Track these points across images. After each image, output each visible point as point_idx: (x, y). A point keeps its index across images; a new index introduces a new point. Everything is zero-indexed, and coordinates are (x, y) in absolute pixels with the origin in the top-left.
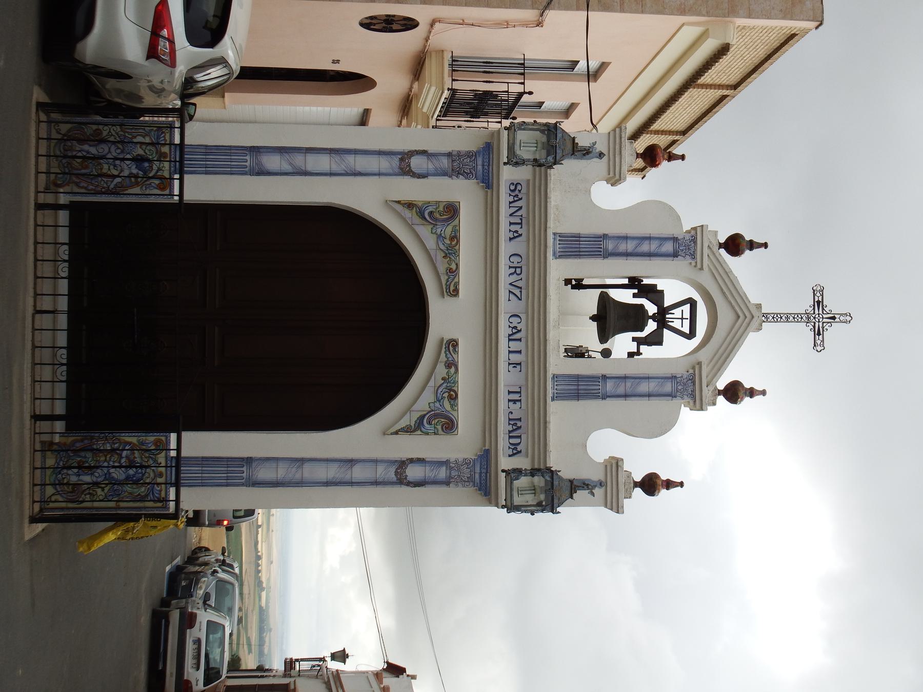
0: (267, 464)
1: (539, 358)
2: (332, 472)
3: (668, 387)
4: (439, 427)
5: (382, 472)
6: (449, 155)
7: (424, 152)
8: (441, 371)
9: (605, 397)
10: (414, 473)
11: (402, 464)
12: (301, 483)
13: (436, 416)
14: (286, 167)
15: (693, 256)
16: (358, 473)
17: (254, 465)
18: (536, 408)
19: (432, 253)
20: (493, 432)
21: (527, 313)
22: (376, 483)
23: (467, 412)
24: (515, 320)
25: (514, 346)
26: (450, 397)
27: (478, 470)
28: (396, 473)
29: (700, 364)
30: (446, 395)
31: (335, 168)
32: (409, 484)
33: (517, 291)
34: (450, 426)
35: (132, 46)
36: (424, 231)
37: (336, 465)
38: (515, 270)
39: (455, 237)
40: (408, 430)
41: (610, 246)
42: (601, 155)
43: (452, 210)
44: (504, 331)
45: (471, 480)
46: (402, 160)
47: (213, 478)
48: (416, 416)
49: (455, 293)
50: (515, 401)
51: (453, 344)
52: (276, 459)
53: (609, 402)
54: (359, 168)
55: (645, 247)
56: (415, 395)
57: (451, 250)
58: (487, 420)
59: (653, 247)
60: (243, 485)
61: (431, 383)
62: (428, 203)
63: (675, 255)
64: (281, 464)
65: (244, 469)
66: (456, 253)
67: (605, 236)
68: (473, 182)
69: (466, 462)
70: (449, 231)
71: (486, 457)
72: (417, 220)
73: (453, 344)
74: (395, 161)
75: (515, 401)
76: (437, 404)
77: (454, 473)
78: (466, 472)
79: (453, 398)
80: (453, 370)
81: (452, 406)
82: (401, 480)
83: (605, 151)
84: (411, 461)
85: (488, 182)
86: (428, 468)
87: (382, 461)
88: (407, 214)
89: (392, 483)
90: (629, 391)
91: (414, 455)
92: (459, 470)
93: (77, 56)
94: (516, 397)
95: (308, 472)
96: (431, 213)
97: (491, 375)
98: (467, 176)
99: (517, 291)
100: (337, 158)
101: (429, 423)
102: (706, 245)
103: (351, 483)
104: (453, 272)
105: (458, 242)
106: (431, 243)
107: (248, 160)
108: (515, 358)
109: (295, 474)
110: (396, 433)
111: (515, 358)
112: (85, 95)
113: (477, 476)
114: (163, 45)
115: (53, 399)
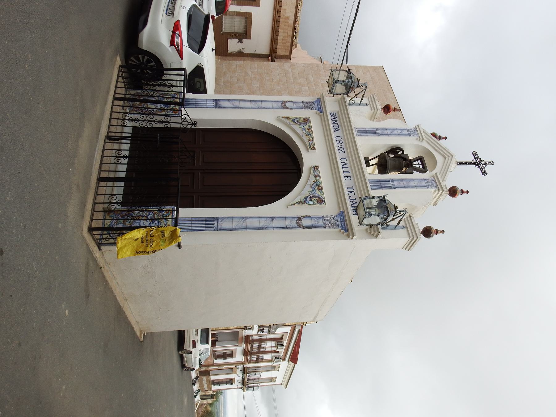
0: (227, 220)
1: (359, 172)
2: (262, 223)
3: (424, 184)
4: (316, 202)
5: (288, 222)
6: (302, 102)
7: (291, 101)
8: (312, 178)
9: (395, 188)
10: (305, 222)
11: (299, 219)
12: (246, 229)
13: (313, 197)
14: (232, 106)
15: (418, 135)
16: (276, 223)
17: (220, 220)
18: (361, 186)
19: (301, 134)
20: (343, 202)
21: (348, 157)
22: (286, 228)
23: (328, 194)
24: (344, 160)
25: (345, 169)
26: (319, 189)
27: (339, 220)
28: (297, 223)
29: (436, 174)
30: (317, 188)
31: (253, 106)
32: (304, 228)
33: (342, 149)
34: (321, 201)
35: (164, 38)
36: (296, 127)
37: (264, 219)
38: (339, 142)
39: (310, 129)
40: (300, 203)
41: (380, 132)
42: (367, 105)
43: (307, 120)
44: (340, 165)
45: (336, 225)
46: (282, 104)
47: (198, 227)
48: (303, 197)
49: (314, 148)
50: (351, 192)
51: (316, 168)
52: (232, 217)
53: (397, 190)
54: (263, 106)
55: (395, 132)
56: (302, 188)
57: (309, 132)
58: (339, 199)
59: (399, 132)
60: (214, 230)
61: (308, 183)
62: (296, 118)
63: (409, 135)
64: (234, 220)
65: (215, 222)
66: (312, 135)
67: (377, 129)
68: (314, 111)
69: (332, 217)
70: (307, 127)
71: (342, 214)
72: (291, 123)
73: (316, 168)
74: (280, 104)
75: (351, 192)
76: (313, 192)
77: (327, 222)
78: (333, 222)
79: (320, 189)
80: (318, 178)
81: (320, 193)
82: (300, 226)
83: (368, 103)
84: (304, 217)
85: (321, 110)
86: (313, 220)
87: (288, 217)
88: (287, 121)
89: (295, 227)
90: (406, 185)
91: (305, 215)
92: (329, 221)
93: (139, 46)
94: (351, 190)
95: (249, 223)
96: (298, 121)
97: (337, 179)
98: (311, 109)
99: (342, 149)
100: (254, 103)
101: (311, 200)
102: (422, 132)
103: (273, 228)
104: (311, 141)
105: (312, 130)
106: (299, 131)
107: (214, 103)
108: (346, 174)
109: (242, 224)
110: (294, 205)
111: (346, 174)
112: (143, 71)
113: (339, 223)
114: (177, 40)
115: (112, 195)
